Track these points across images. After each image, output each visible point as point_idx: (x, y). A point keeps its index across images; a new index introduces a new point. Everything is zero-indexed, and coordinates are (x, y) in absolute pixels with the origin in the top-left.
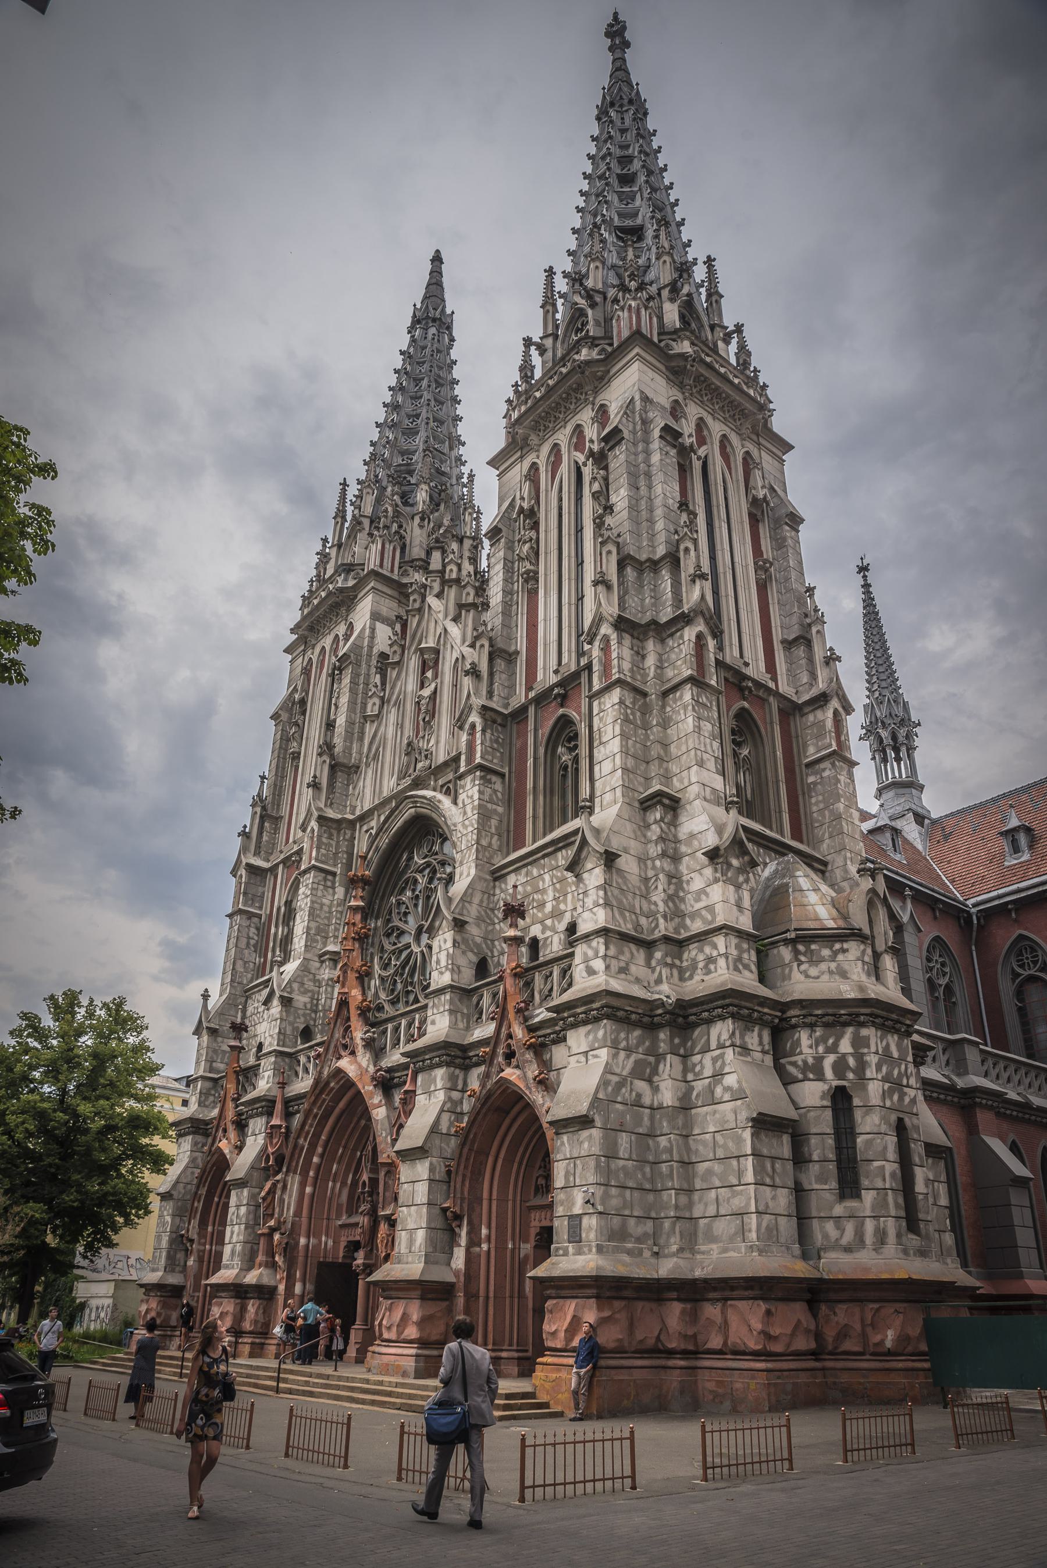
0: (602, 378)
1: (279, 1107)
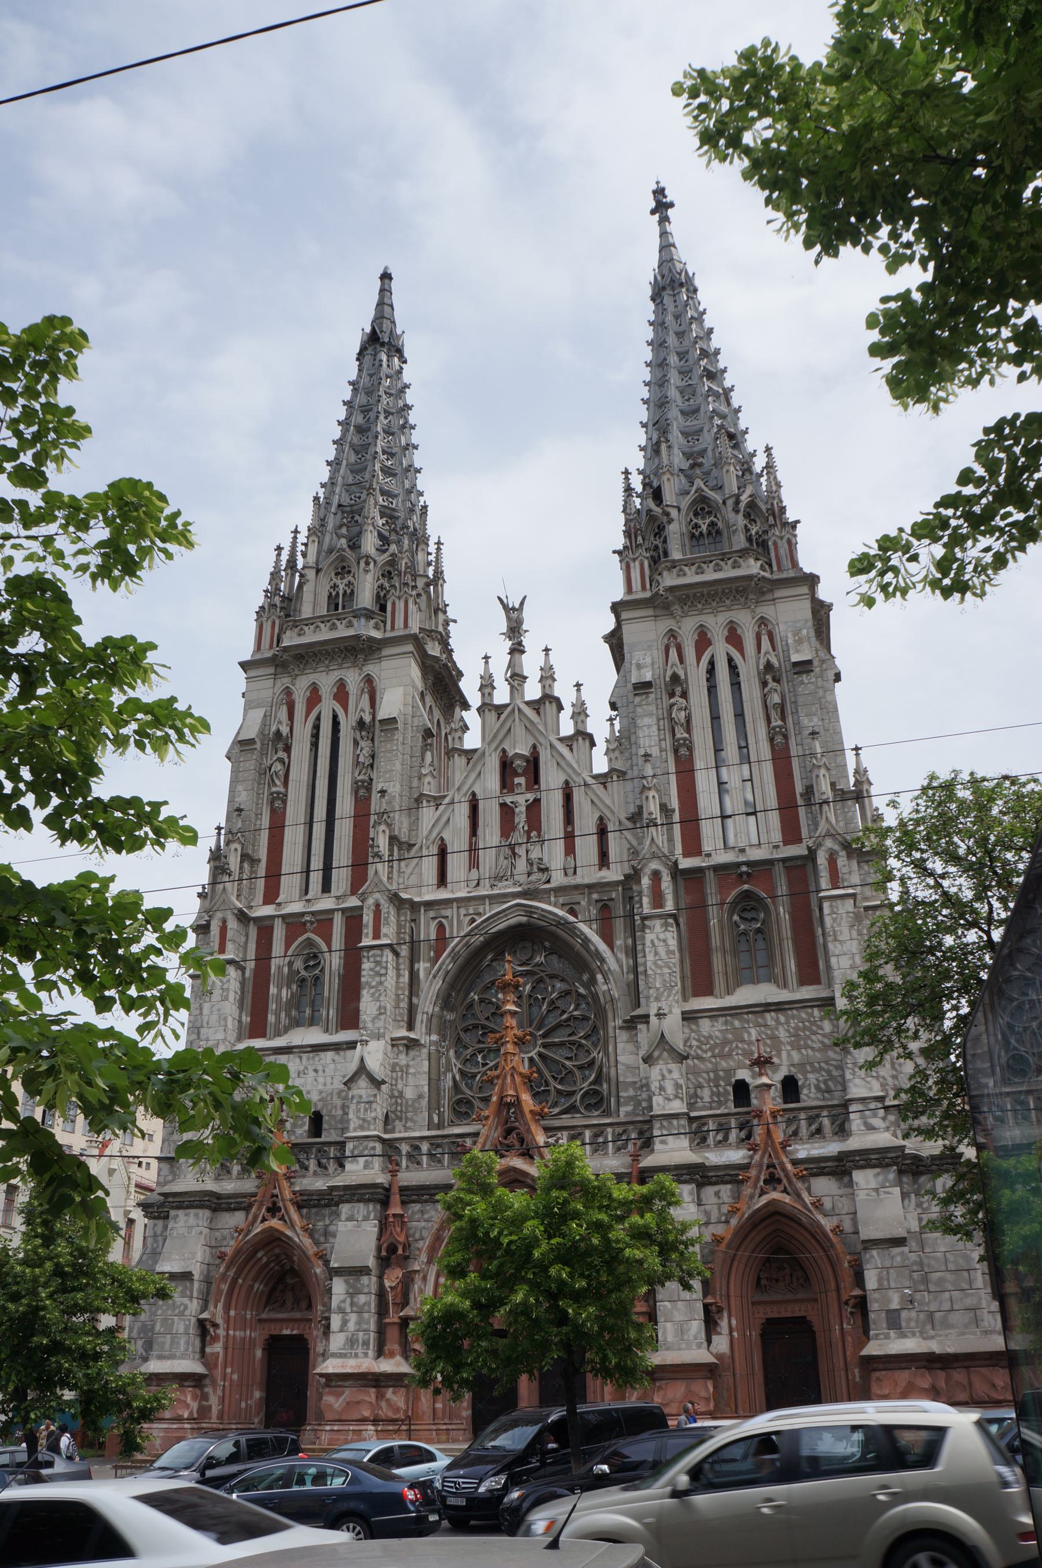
0: (763, 593)
1: (396, 1198)
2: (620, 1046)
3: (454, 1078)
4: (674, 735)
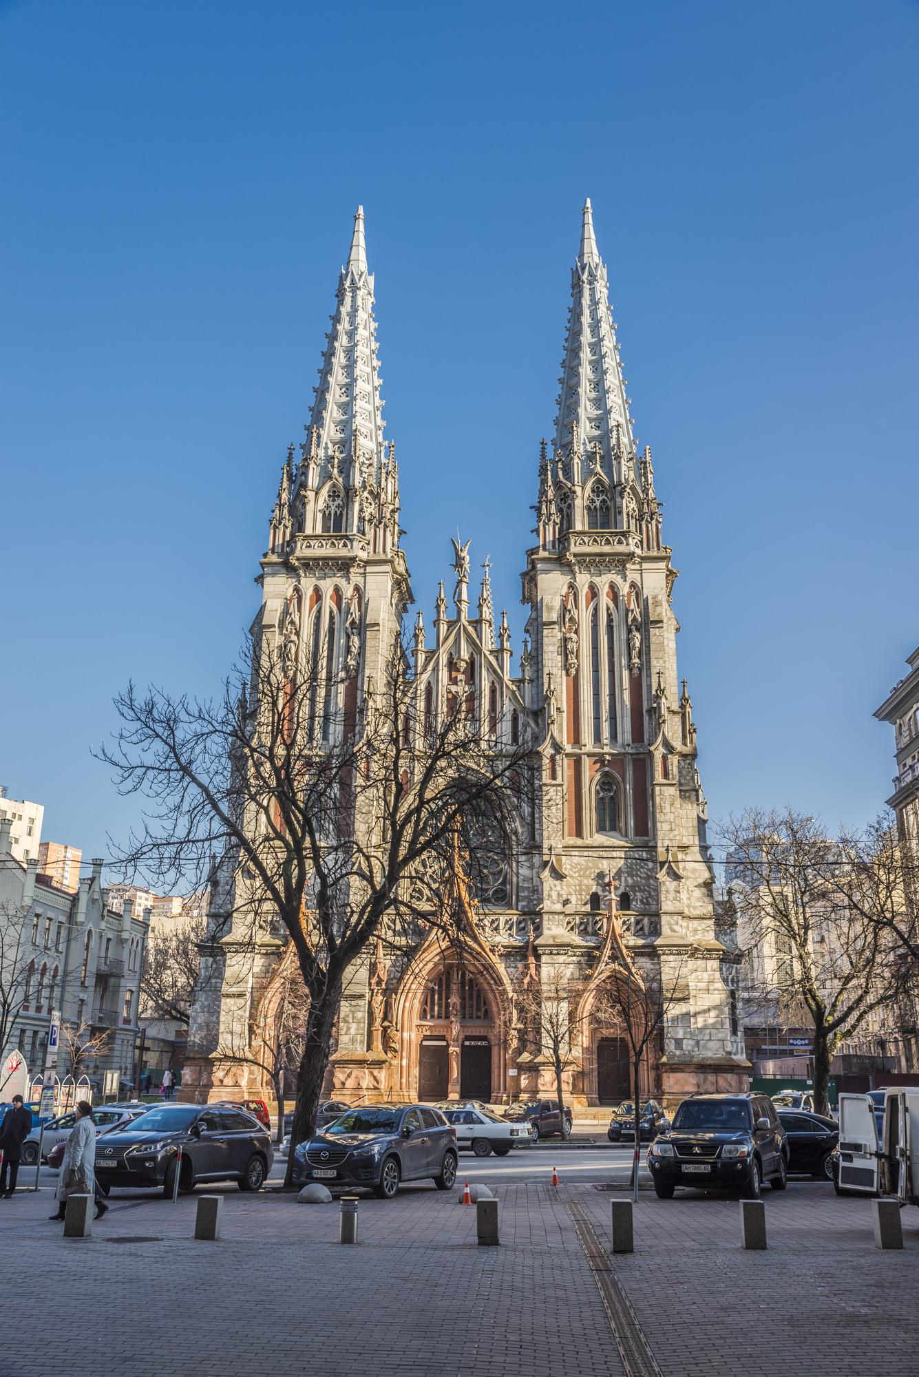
4: (566, 659)
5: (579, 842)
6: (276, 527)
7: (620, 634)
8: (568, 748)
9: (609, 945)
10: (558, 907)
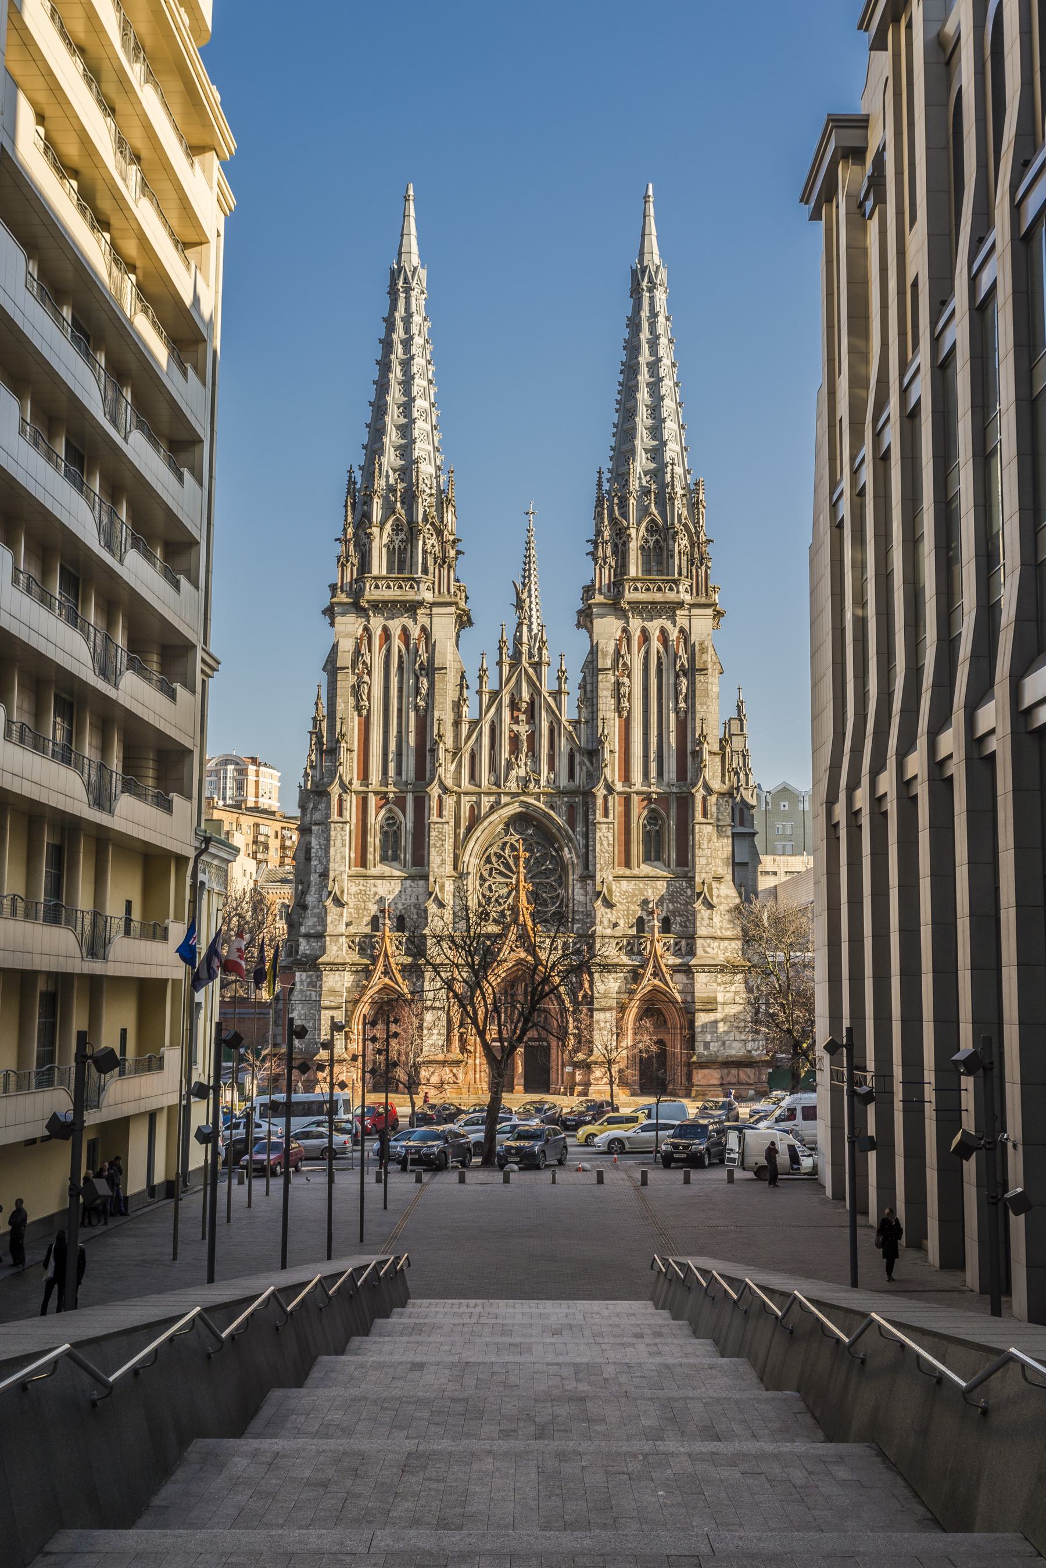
2: (576, 890)
3: (478, 897)
4: (619, 702)
5: (628, 872)
6: (343, 565)
7: (669, 679)
8: (619, 787)
9: (652, 962)
10: (608, 932)
